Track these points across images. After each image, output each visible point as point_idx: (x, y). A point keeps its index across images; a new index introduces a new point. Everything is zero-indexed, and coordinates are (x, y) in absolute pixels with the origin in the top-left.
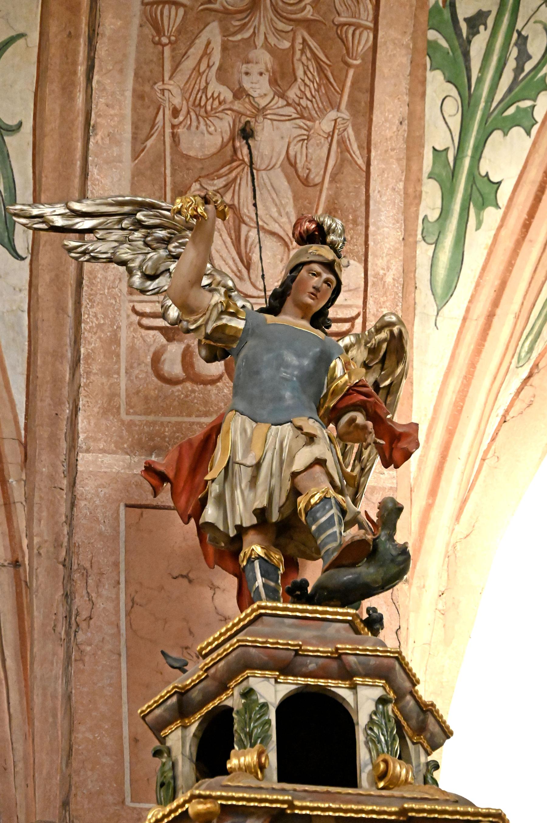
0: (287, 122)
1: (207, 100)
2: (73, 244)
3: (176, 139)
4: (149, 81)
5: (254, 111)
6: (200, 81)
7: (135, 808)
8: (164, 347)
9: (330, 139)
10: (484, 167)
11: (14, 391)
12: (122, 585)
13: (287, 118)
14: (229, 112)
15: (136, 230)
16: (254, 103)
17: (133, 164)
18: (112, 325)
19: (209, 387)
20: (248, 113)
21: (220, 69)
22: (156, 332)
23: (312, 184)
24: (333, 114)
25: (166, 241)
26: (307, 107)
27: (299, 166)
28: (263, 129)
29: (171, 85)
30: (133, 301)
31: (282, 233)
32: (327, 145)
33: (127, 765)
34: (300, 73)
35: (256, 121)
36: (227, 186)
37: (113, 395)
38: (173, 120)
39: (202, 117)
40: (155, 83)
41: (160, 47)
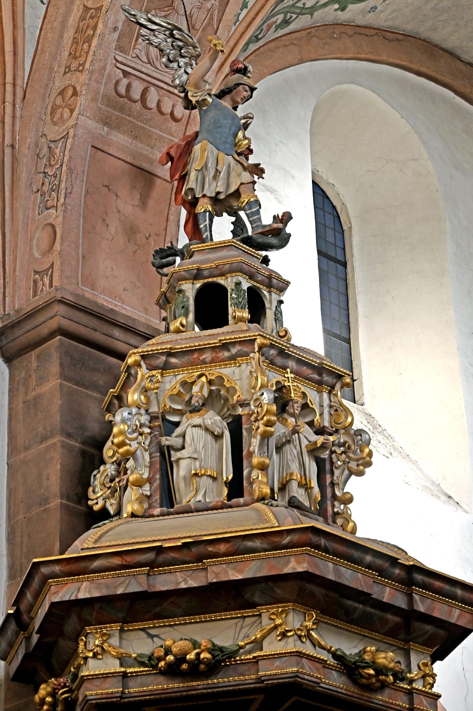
2: (144, 33)
7: (82, 289)
8: (121, 78)
11: (26, 64)
12: (85, 182)
15: (169, 37)
18: (105, 61)
19: (133, 103)
22: (120, 71)
25: (181, 48)
27: (193, 18)
30: (115, 53)
33: (80, 267)
37: (98, 93)
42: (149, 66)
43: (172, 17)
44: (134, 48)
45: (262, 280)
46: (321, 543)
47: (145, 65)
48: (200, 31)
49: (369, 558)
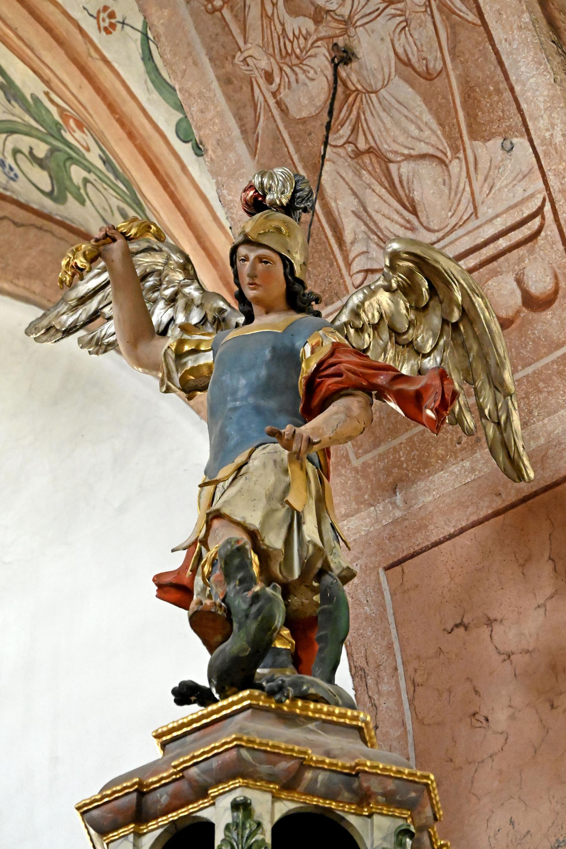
0: (379, 18)
1: (292, 42)
3: (283, 107)
4: (227, 59)
5: (341, 26)
6: (275, 26)
9: (428, 10)
13: (376, 13)
14: (319, 43)
16: (336, 17)
17: (255, 162)
20: (338, 32)
23: (435, 75)
27: (414, 60)
28: (359, 41)
29: (249, 49)
31: (431, 151)
32: (429, 19)
35: (349, 36)
36: (354, 130)
38: (270, 87)
39: (296, 65)
40: (234, 57)
41: (217, 14)
43: (368, 113)
44: (349, 265)
45: (174, 796)
48: (450, 66)
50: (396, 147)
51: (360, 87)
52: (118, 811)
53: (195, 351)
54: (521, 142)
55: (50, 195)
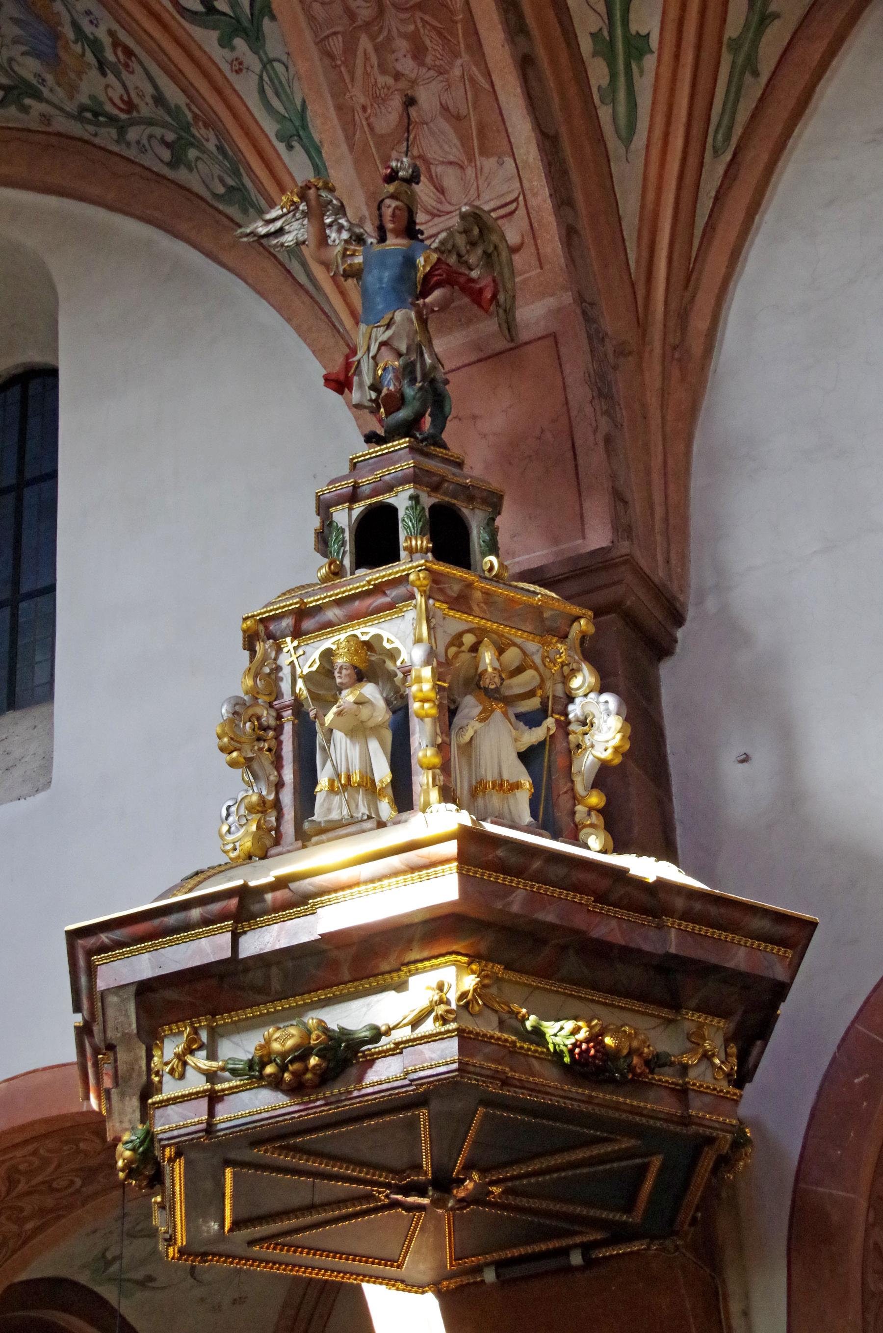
10: (634, 28)
14: (396, 92)
21: (379, 66)
24: (459, 62)
26: (441, 65)
31: (455, 160)
34: (428, 42)
42: (437, 220)
46: (103, 942)
47: (430, 224)
49: (195, 913)
50: (436, 156)
51: (417, 120)
52: (339, 496)
53: (353, 255)
54: (508, 161)
55: (169, 164)
